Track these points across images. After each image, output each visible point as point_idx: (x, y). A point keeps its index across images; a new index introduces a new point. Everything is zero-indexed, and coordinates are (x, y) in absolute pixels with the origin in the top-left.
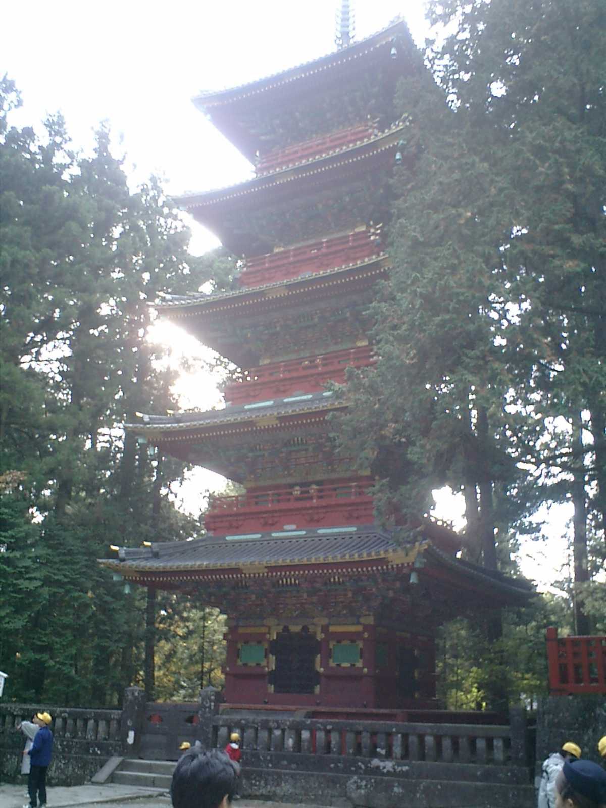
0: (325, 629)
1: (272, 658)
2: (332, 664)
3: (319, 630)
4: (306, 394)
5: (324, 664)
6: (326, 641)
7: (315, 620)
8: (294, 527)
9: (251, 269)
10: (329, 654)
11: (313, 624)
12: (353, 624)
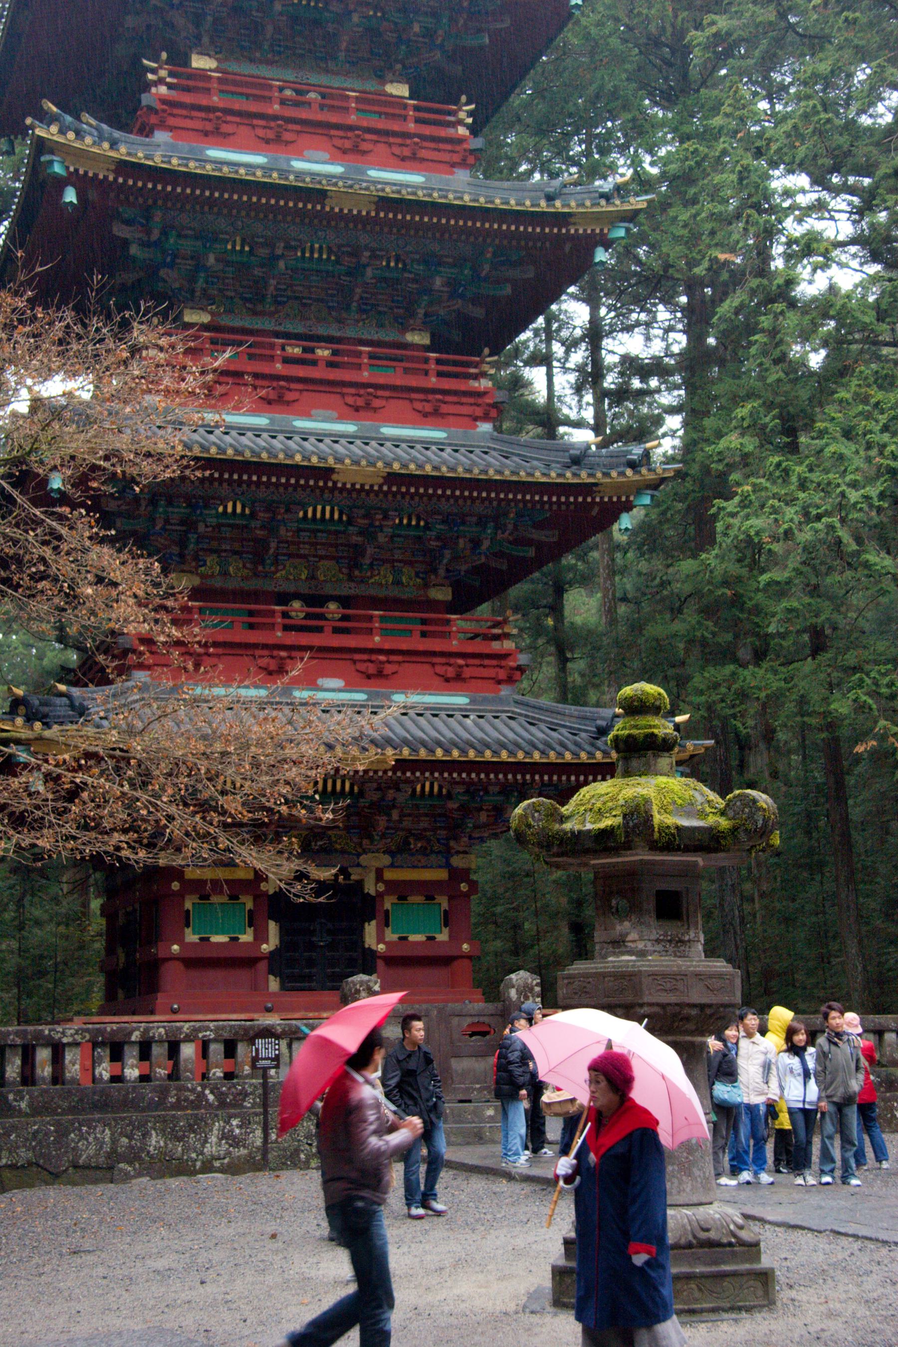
0: (379, 876)
1: (273, 928)
2: (391, 936)
3: (372, 876)
4: (341, 418)
5: (380, 940)
6: (380, 895)
7: (364, 859)
8: (338, 683)
9: (173, 93)
10: (386, 922)
11: (359, 865)
12: (440, 867)
